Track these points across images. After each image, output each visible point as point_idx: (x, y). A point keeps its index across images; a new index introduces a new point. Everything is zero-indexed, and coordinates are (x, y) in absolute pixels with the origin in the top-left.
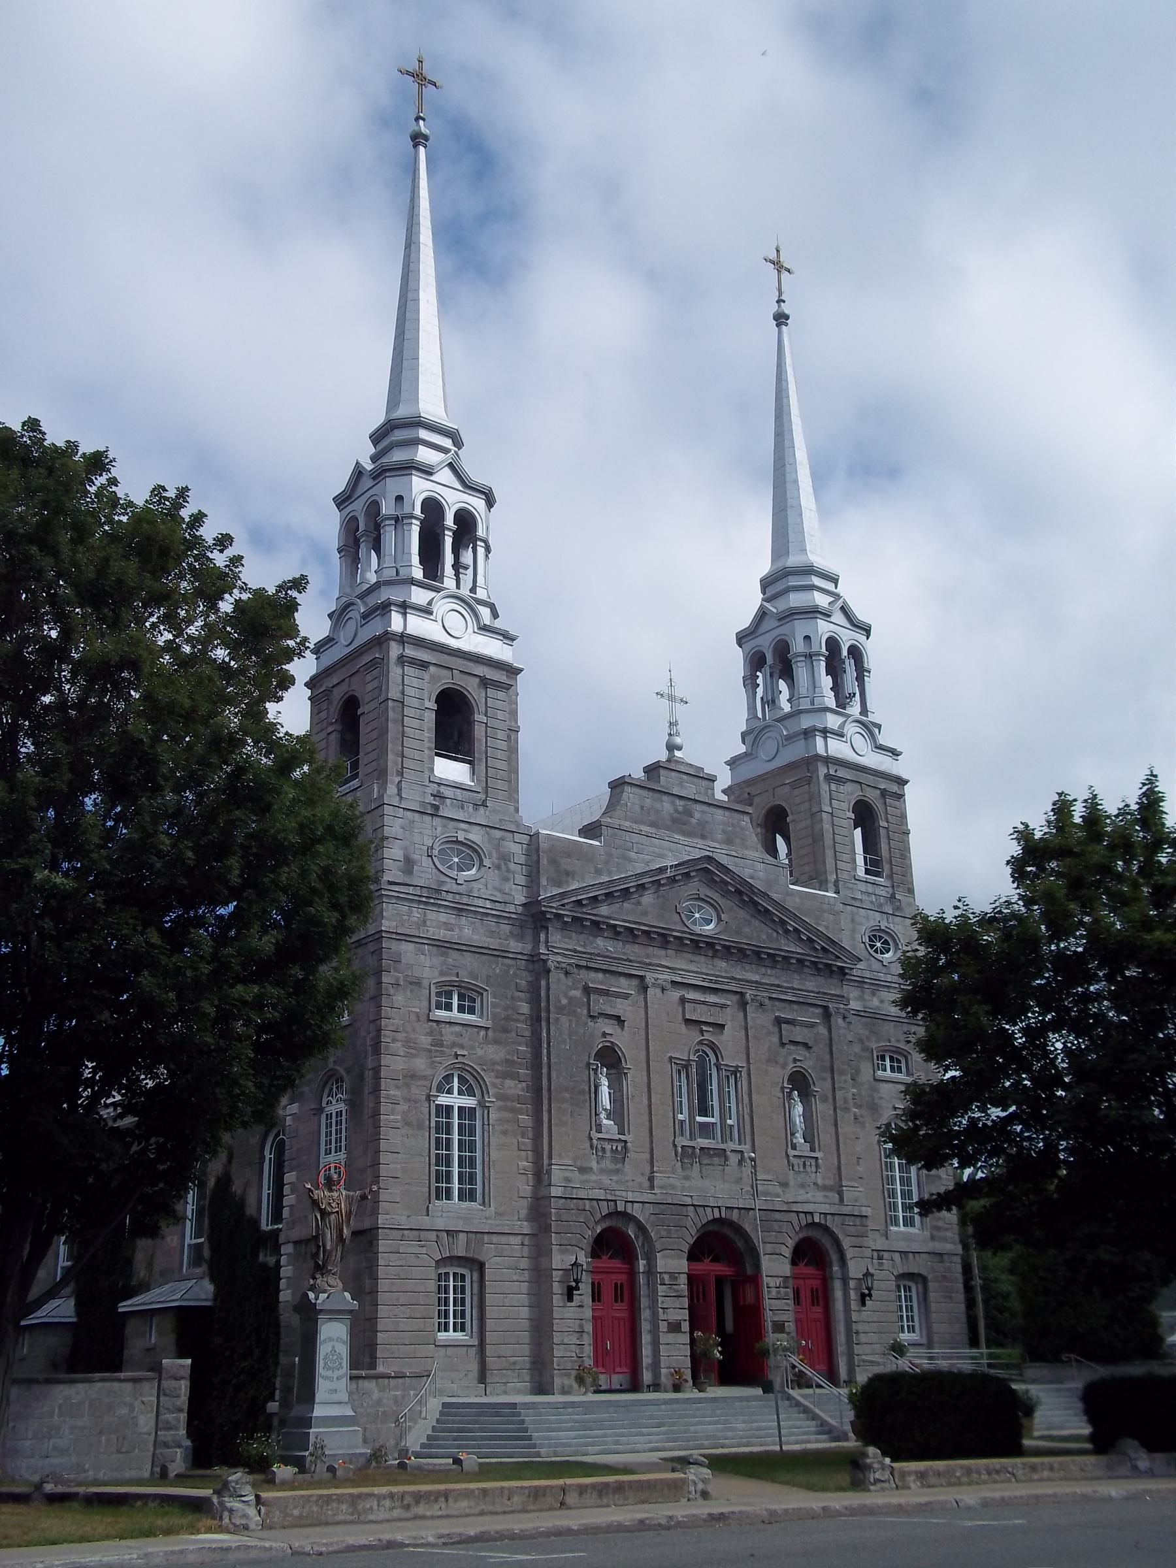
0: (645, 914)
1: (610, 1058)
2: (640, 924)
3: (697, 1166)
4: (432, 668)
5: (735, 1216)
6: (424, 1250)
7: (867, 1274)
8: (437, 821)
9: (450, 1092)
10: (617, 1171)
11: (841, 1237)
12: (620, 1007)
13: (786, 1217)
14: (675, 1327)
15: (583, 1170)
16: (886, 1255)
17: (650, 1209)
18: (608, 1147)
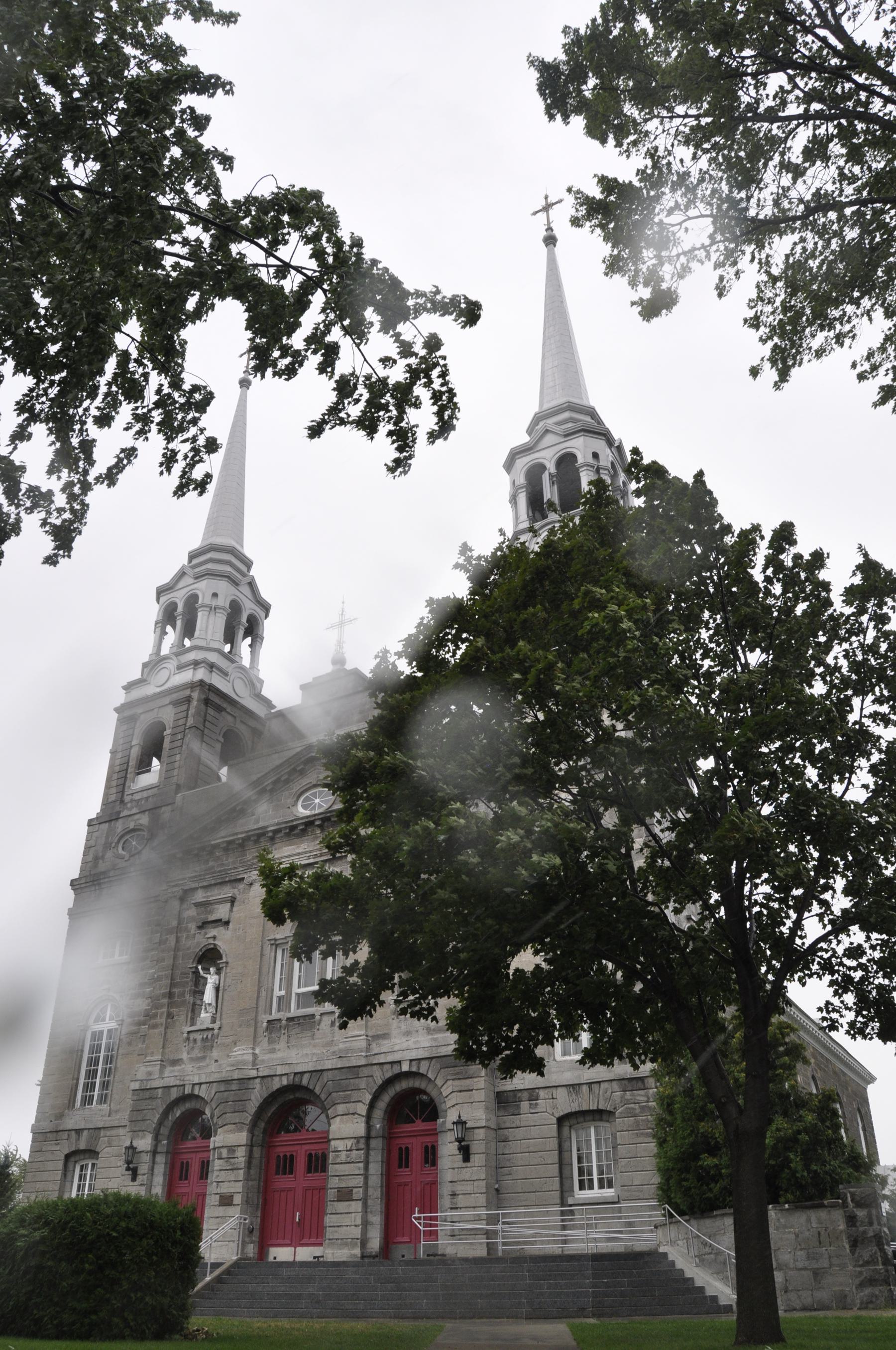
0: (257, 821)
1: (210, 957)
2: (237, 834)
3: (284, 1038)
4: (142, 717)
5: (305, 1082)
6: (58, 1148)
7: (460, 1123)
8: (120, 821)
9: (104, 1020)
10: (203, 1058)
11: (439, 1082)
12: (222, 911)
13: (365, 1071)
14: (226, 1201)
15: (175, 1062)
16: (542, 1093)
17: (215, 1086)
18: (199, 1037)
